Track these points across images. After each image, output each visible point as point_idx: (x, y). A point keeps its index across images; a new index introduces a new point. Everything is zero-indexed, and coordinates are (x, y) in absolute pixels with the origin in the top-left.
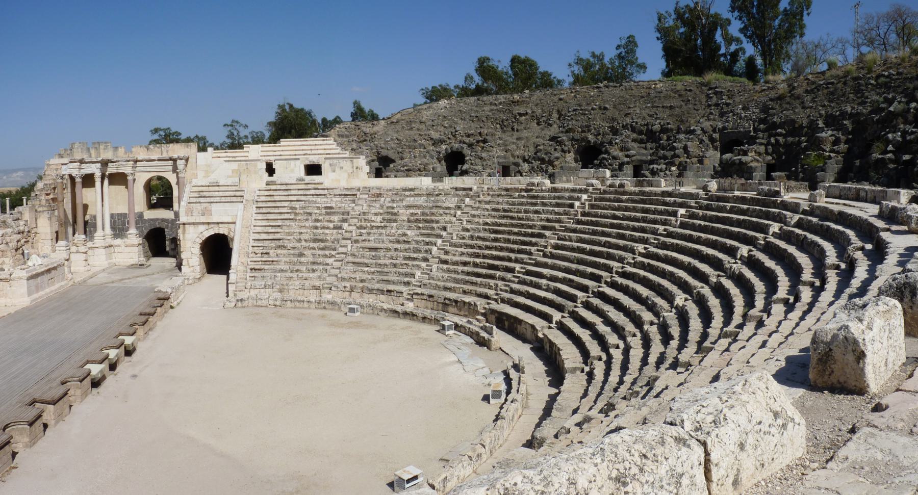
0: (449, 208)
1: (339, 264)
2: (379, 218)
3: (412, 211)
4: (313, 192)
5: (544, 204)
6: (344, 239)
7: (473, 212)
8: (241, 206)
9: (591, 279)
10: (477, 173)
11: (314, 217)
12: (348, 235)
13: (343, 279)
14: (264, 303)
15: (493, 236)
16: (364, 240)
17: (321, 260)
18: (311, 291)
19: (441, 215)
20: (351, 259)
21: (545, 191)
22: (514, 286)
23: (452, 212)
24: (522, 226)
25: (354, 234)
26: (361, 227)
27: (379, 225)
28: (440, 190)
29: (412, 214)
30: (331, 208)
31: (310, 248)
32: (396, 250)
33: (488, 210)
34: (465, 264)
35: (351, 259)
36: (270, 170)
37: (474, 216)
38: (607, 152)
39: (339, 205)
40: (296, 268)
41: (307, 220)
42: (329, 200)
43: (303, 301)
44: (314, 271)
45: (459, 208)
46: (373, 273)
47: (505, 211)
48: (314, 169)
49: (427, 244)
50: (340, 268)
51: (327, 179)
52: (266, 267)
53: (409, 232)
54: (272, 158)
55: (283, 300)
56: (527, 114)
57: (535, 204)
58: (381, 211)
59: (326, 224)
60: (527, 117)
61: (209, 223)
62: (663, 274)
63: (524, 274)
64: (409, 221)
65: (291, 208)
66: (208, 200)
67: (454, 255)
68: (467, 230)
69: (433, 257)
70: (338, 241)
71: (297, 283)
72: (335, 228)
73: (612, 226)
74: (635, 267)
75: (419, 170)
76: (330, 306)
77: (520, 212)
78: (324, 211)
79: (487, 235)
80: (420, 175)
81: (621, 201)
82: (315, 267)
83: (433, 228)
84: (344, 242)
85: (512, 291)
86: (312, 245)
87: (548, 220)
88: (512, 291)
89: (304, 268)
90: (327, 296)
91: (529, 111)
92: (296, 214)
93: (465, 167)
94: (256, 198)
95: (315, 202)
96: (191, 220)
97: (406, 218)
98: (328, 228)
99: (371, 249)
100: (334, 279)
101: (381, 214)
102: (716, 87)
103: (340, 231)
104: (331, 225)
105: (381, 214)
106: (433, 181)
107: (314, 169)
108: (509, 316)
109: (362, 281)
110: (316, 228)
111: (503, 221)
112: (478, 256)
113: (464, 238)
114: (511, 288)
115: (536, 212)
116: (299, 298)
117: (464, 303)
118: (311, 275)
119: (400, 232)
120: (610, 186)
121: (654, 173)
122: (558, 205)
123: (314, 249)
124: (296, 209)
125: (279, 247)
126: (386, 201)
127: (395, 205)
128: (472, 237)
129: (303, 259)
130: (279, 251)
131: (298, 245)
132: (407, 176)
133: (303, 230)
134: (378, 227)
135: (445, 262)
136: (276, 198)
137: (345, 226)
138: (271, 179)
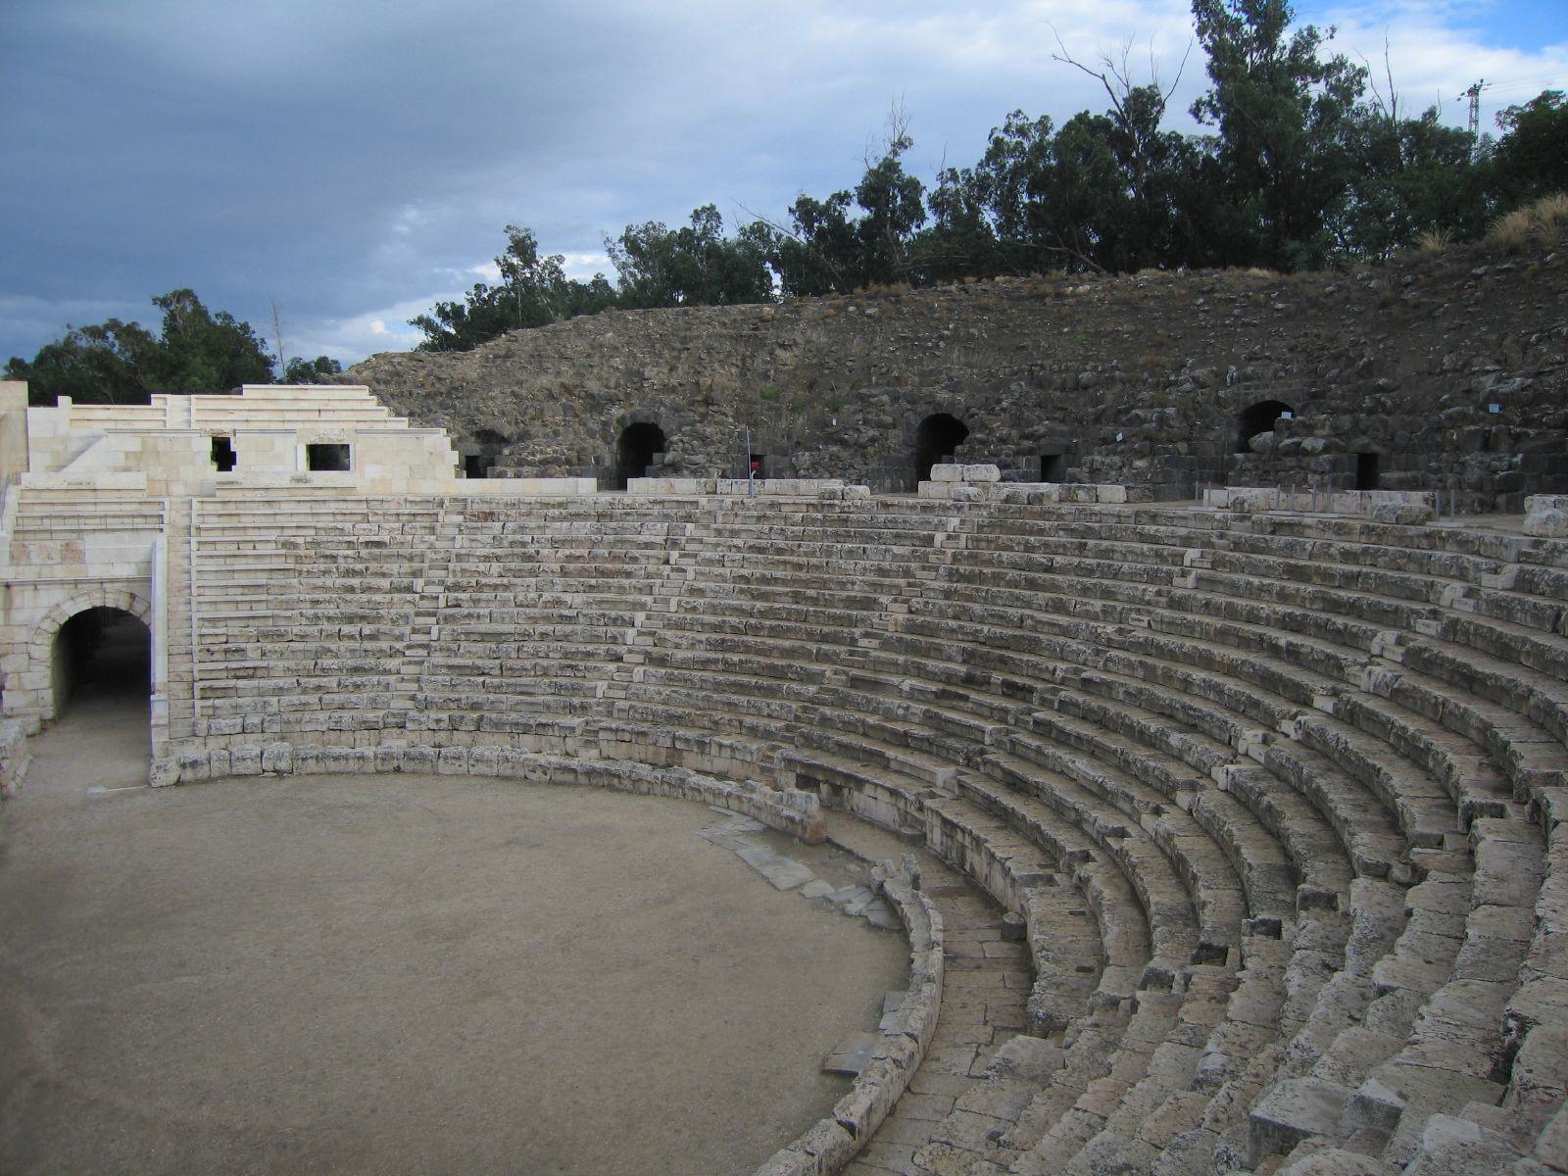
0: (648, 545)
1: (413, 669)
2: (496, 567)
4: (333, 507)
6: (418, 614)
7: (708, 554)
8: (161, 540)
10: (697, 471)
11: (343, 565)
12: (426, 605)
13: (427, 705)
14: (251, 767)
15: (760, 605)
16: (470, 616)
17: (371, 661)
18: (358, 735)
20: (438, 658)
22: (827, 711)
23: (662, 553)
25: (442, 603)
27: (498, 581)
29: (570, 558)
30: (379, 544)
31: (340, 636)
32: (544, 636)
35: (438, 658)
36: (223, 455)
37: (710, 562)
38: (983, 427)
39: (400, 538)
40: (314, 681)
43: (346, 758)
45: (675, 544)
46: (498, 688)
47: (780, 551)
48: (325, 457)
49: (615, 621)
50: (418, 680)
51: (364, 476)
52: (241, 683)
53: (568, 598)
54: (225, 428)
55: (294, 757)
56: (796, 344)
58: (499, 552)
59: (375, 582)
60: (796, 351)
61: (76, 583)
64: (564, 573)
65: (285, 545)
66: (72, 524)
67: (677, 646)
69: (630, 651)
70: (406, 617)
71: (322, 716)
72: (395, 589)
73: (1032, 584)
75: (568, 462)
78: (364, 552)
79: (745, 603)
80: (570, 474)
81: (1041, 532)
82: (357, 679)
83: (622, 590)
84: (421, 621)
86: (347, 629)
89: (331, 682)
90: (396, 743)
91: (800, 340)
92: (298, 559)
93: (669, 457)
94: (196, 521)
96: (29, 574)
97: (556, 567)
98: (378, 590)
99: (485, 637)
100: (410, 704)
101: (498, 558)
102: (1212, 291)
103: (409, 597)
104: (385, 583)
105: (498, 558)
106: (600, 488)
107: (325, 457)
109: (475, 707)
111: (779, 574)
112: (733, 648)
116: (336, 750)
117: (721, 746)
118: (354, 697)
119: (547, 596)
120: (1008, 500)
121: (1096, 475)
123: (351, 637)
124: (295, 546)
125: (266, 635)
129: (327, 662)
130: (269, 646)
131: (314, 630)
132: (542, 475)
133: (321, 596)
134: (495, 587)
136: (247, 521)
137: (419, 584)
138: (225, 475)
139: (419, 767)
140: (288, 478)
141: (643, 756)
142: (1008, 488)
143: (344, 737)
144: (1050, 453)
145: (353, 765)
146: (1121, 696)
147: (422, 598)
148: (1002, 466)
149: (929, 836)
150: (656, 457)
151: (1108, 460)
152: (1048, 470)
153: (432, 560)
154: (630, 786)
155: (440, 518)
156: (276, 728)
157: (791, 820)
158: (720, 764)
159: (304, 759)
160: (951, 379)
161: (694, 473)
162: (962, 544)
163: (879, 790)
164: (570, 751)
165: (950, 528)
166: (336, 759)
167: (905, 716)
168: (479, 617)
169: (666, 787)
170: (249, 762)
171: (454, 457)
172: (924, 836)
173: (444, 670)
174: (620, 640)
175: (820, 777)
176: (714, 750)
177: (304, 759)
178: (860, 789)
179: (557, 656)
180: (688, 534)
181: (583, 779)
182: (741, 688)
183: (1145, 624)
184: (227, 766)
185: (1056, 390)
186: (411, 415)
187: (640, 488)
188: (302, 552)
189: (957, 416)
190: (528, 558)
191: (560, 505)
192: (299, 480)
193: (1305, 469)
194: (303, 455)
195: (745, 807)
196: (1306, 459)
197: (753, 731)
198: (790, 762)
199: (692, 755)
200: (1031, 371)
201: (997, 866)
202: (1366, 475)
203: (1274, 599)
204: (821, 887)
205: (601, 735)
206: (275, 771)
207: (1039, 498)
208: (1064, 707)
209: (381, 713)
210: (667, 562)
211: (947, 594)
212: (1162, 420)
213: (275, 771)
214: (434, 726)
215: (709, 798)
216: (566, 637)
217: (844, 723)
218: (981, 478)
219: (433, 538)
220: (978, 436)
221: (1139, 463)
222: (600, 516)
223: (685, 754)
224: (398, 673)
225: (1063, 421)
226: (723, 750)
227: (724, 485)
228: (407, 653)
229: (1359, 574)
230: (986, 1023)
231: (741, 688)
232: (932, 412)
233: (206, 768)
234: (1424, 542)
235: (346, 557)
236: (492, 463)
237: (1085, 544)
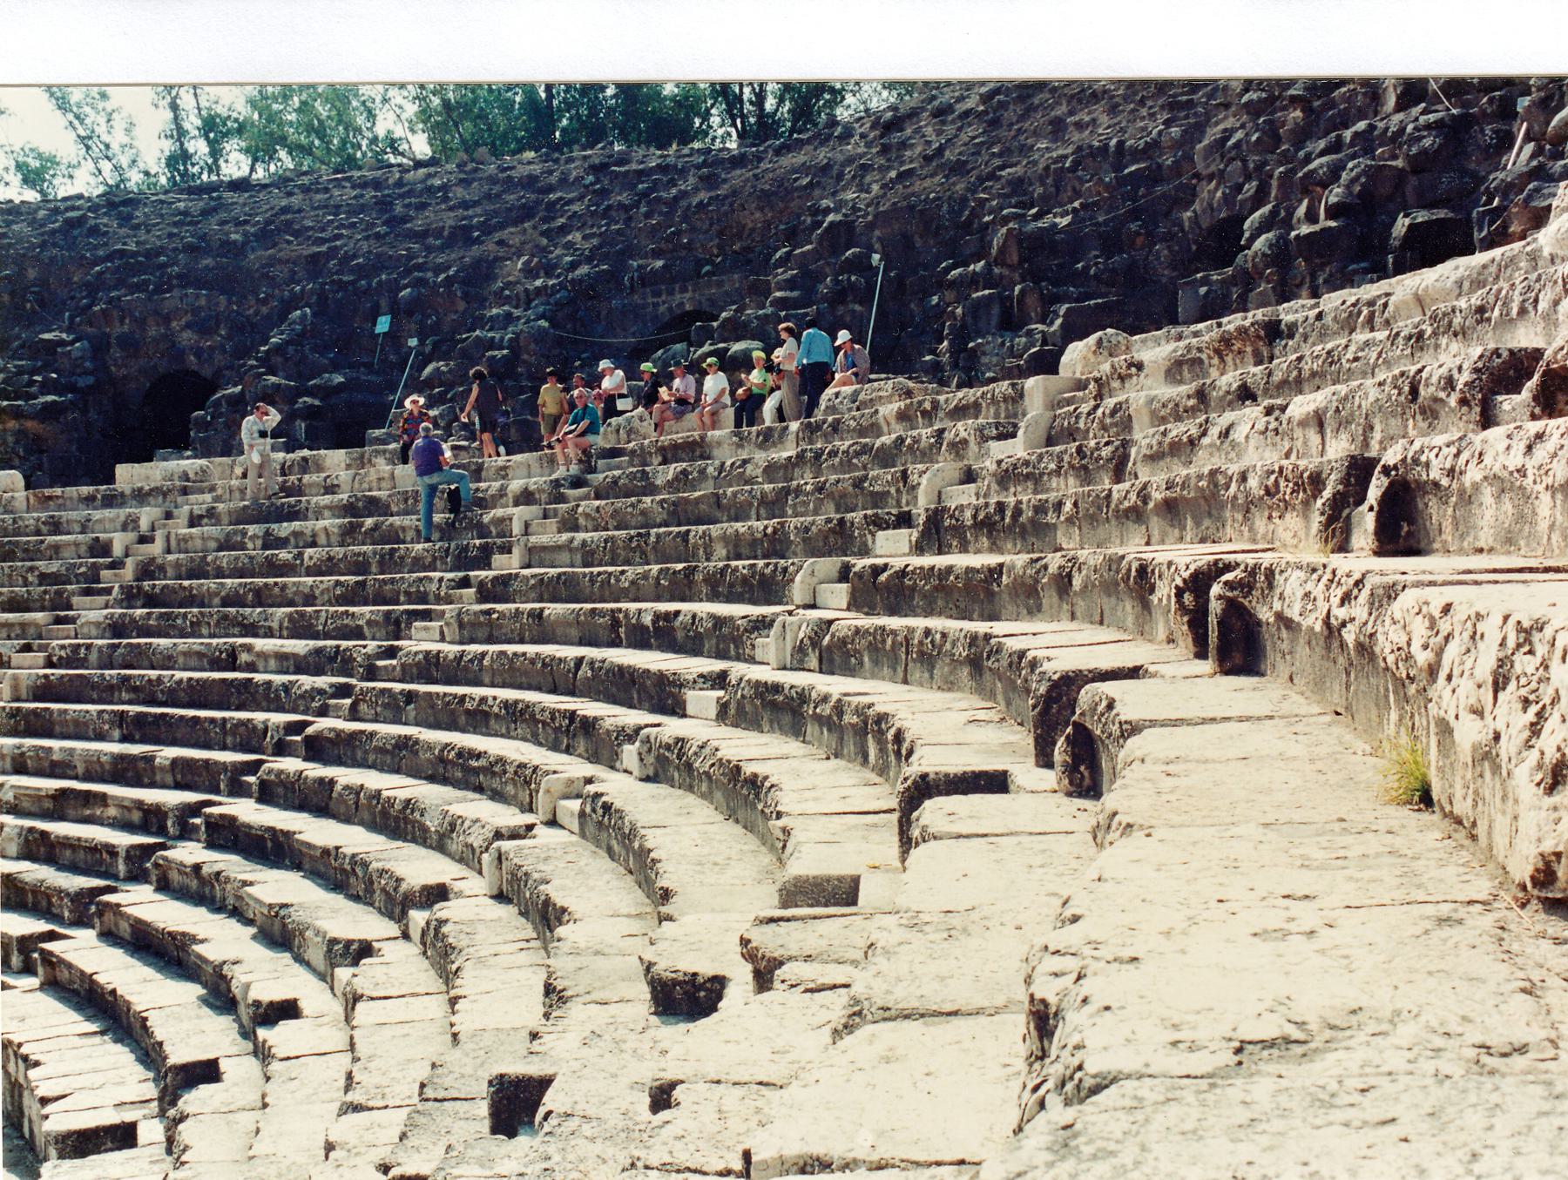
74: (354, 715)
165: (144, 524)
211: (117, 629)
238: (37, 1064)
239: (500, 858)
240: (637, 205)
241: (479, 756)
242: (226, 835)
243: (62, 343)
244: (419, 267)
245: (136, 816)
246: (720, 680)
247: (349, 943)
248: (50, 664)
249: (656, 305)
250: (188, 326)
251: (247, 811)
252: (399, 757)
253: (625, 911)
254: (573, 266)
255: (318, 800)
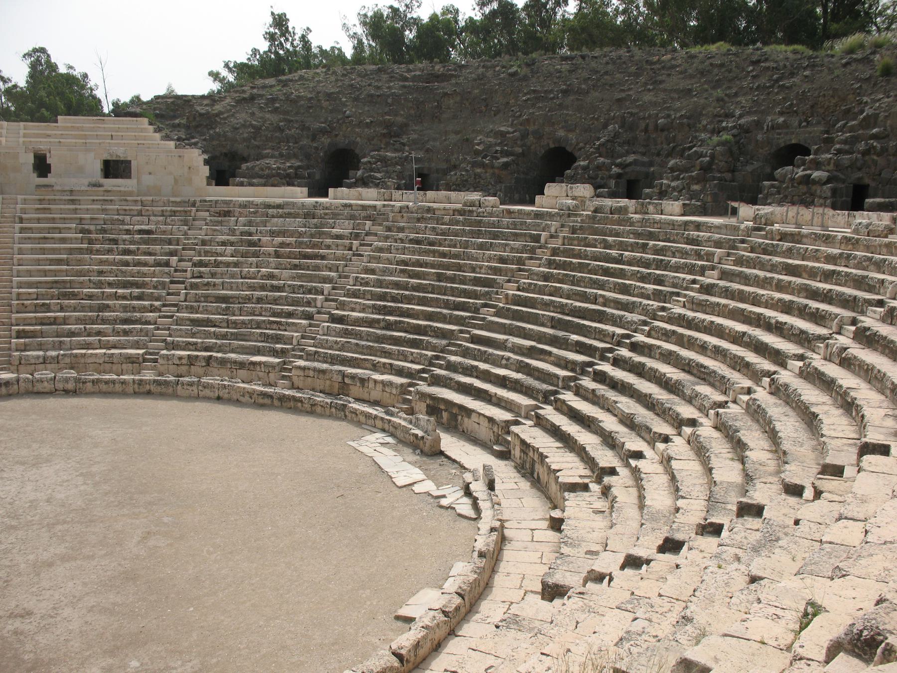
0: (338, 237)
2: (230, 249)
3: (280, 239)
5: (495, 236)
6: (172, 282)
9: (578, 352)
12: (178, 276)
13: (175, 346)
14: (47, 386)
18: (124, 366)
19: (328, 247)
21: (491, 215)
24: (459, 268)
25: (189, 274)
26: (201, 264)
28: (327, 208)
29: (282, 245)
30: (148, 232)
32: (259, 300)
33: (402, 241)
34: (371, 323)
36: (42, 166)
37: (381, 250)
41: (109, 251)
42: (146, 219)
43: (113, 382)
44: (126, 333)
45: (357, 236)
46: (224, 336)
47: (432, 244)
50: (169, 329)
57: (479, 234)
62: (703, 348)
63: (466, 340)
67: (353, 310)
68: (373, 271)
70: (164, 283)
72: (158, 264)
73: (606, 272)
74: (649, 335)
76: (159, 389)
77: (455, 246)
85: (450, 367)
87: (502, 260)
88: (450, 367)
92: (90, 242)
95: (123, 222)
98: (145, 264)
103: (166, 269)
107: (114, 168)
108: (449, 404)
110: (127, 264)
113: (367, 284)
114: (449, 362)
115: (481, 247)
117: (375, 381)
121: (663, 194)
122: (516, 237)
124: (89, 232)
125: (66, 296)
126: (239, 223)
127: (253, 229)
128: (380, 284)
134: (228, 265)
135: (340, 320)
139: (164, 390)
140: (87, 183)
141: (322, 387)
142: (599, 202)
143: (115, 367)
144: (632, 178)
145: (118, 388)
146: (657, 356)
147: (176, 271)
148: (596, 187)
149: (513, 452)
150: (351, 173)
151: (673, 184)
152: (631, 190)
153: (184, 244)
154: (309, 409)
155: (193, 214)
156: (67, 360)
157: (416, 436)
158: (376, 394)
159: (84, 383)
160: (566, 122)
161: (377, 186)
162: (560, 241)
163: (481, 417)
164: (272, 383)
166: (107, 382)
167: (506, 365)
168: (214, 285)
169: (333, 410)
170: (46, 384)
171: (206, 171)
172: (510, 451)
173: (188, 323)
174: (313, 304)
175: (442, 407)
176: (371, 385)
177: (84, 383)
178: (469, 417)
179: (268, 314)
180: (367, 228)
181: (276, 402)
182: (396, 341)
183: (682, 304)
184: (30, 386)
185: (642, 131)
186: (179, 139)
187: (338, 197)
188: (93, 236)
189: (569, 149)
190: (252, 244)
191: (279, 206)
192: (95, 185)
193: (813, 195)
194: (98, 166)
195: (386, 426)
196: (814, 187)
197: (400, 372)
198: (423, 396)
199: (356, 388)
200: (623, 118)
201: (552, 476)
202: (855, 199)
203: (774, 288)
204: (428, 486)
205: (293, 371)
206: (64, 390)
207: (622, 210)
208: (617, 362)
209: (141, 352)
210: (350, 249)
212: (713, 157)
213: (64, 390)
214: (178, 362)
215: (362, 419)
216: (276, 301)
217: (463, 368)
218: (581, 195)
219: (186, 227)
220: (582, 163)
221: (696, 187)
222: (307, 216)
223: (351, 387)
224: (155, 324)
225: (644, 154)
226: (378, 385)
227: (397, 194)
228: (164, 309)
229: (834, 271)
230: (521, 587)
231: (396, 341)
232: (552, 146)
233: (16, 387)
234: (884, 250)
235: (124, 241)
236: (234, 176)
237: (647, 244)
238: (547, 457)
239: (717, 414)
240: (772, 86)
241: (705, 367)
242: (601, 377)
243: (508, 133)
244: (668, 108)
245: (563, 362)
246: (801, 358)
247: (661, 434)
248: (519, 290)
249: (778, 139)
250: (563, 127)
251: (606, 367)
252: (668, 358)
253: (766, 448)
254: (741, 116)
255: (639, 370)
